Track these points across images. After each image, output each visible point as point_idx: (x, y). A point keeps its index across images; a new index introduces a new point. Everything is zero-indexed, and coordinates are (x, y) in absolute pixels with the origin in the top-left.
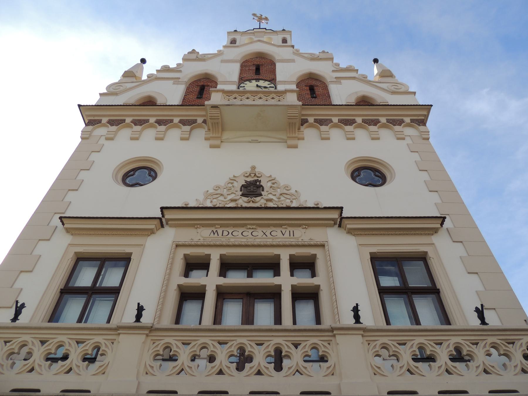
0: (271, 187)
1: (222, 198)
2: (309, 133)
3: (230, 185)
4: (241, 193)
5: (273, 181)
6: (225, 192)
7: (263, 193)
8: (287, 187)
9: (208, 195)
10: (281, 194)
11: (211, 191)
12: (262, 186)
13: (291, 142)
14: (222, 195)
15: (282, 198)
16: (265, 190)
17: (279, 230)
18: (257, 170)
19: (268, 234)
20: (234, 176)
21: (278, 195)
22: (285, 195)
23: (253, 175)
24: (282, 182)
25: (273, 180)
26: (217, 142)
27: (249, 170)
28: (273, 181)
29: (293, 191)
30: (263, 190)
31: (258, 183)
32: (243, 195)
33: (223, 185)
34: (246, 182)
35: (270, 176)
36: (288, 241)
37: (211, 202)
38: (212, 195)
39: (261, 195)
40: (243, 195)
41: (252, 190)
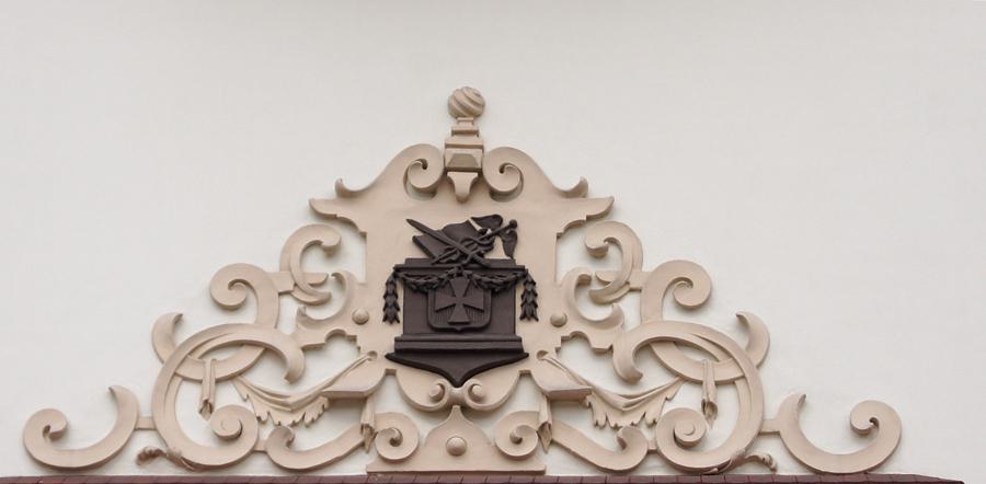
0: (583, 282)
1: (267, 377)
3: (317, 266)
4: (386, 337)
5: (596, 237)
6: (286, 332)
7: (528, 333)
9: (184, 355)
10: (646, 348)
11: (201, 319)
12: (522, 275)
14: (269, 351)
15: (653, 378)
16: (548, 306)
18: (495, 134)
20: (345, 194)
21: (625, 347)
22: (667, 355)
23: (463, 181)
24: (659, 244)
25: (590, 216)
27: (436, 132)
28: (596, 237)
29: (718, 320)
30: (530, 314)
31: (498, 254)
32: (404, 355)
33: (271, 265)
34: (425, 237)
35: (579, 191)
37: (207, 407)
38: (206, 347)
39: (516, 354)
40: (404, 355)
41: (459, 315)
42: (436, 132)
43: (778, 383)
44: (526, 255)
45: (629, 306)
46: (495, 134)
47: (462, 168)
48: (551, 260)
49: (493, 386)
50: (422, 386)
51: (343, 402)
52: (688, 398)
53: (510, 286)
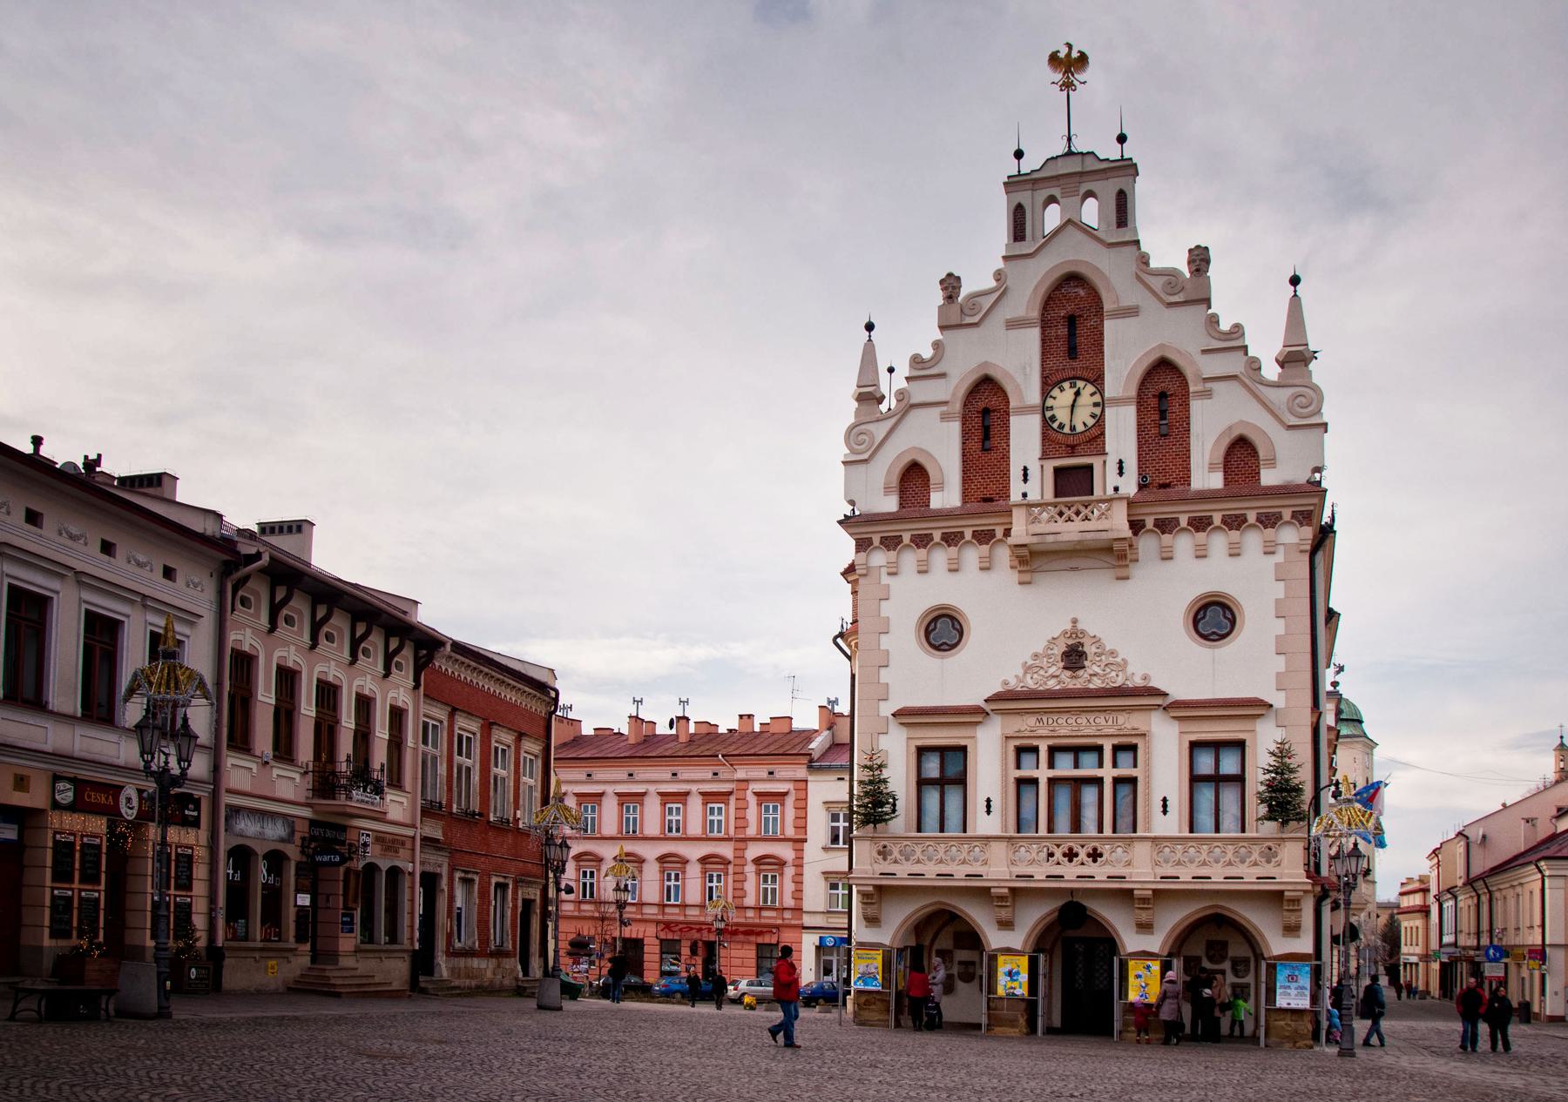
2: (1147, 544)
4: (1061, 664)
8: (1113, 653)
9: (1027, 669)
11: (1030, 662)
13: (1122, 572)
17: (1102, 716)
18: (1080, 626)
25: (1097, 641)
26: (1026, 577)
29: (1119, 660)
38: (1030, 667)
42: (1068, 626)
43: (1130, 669)
46: (1080, 626)
47: (1075, 632)
48: (1090, 649)
49: (1081, 672)
50: (1068, 673)
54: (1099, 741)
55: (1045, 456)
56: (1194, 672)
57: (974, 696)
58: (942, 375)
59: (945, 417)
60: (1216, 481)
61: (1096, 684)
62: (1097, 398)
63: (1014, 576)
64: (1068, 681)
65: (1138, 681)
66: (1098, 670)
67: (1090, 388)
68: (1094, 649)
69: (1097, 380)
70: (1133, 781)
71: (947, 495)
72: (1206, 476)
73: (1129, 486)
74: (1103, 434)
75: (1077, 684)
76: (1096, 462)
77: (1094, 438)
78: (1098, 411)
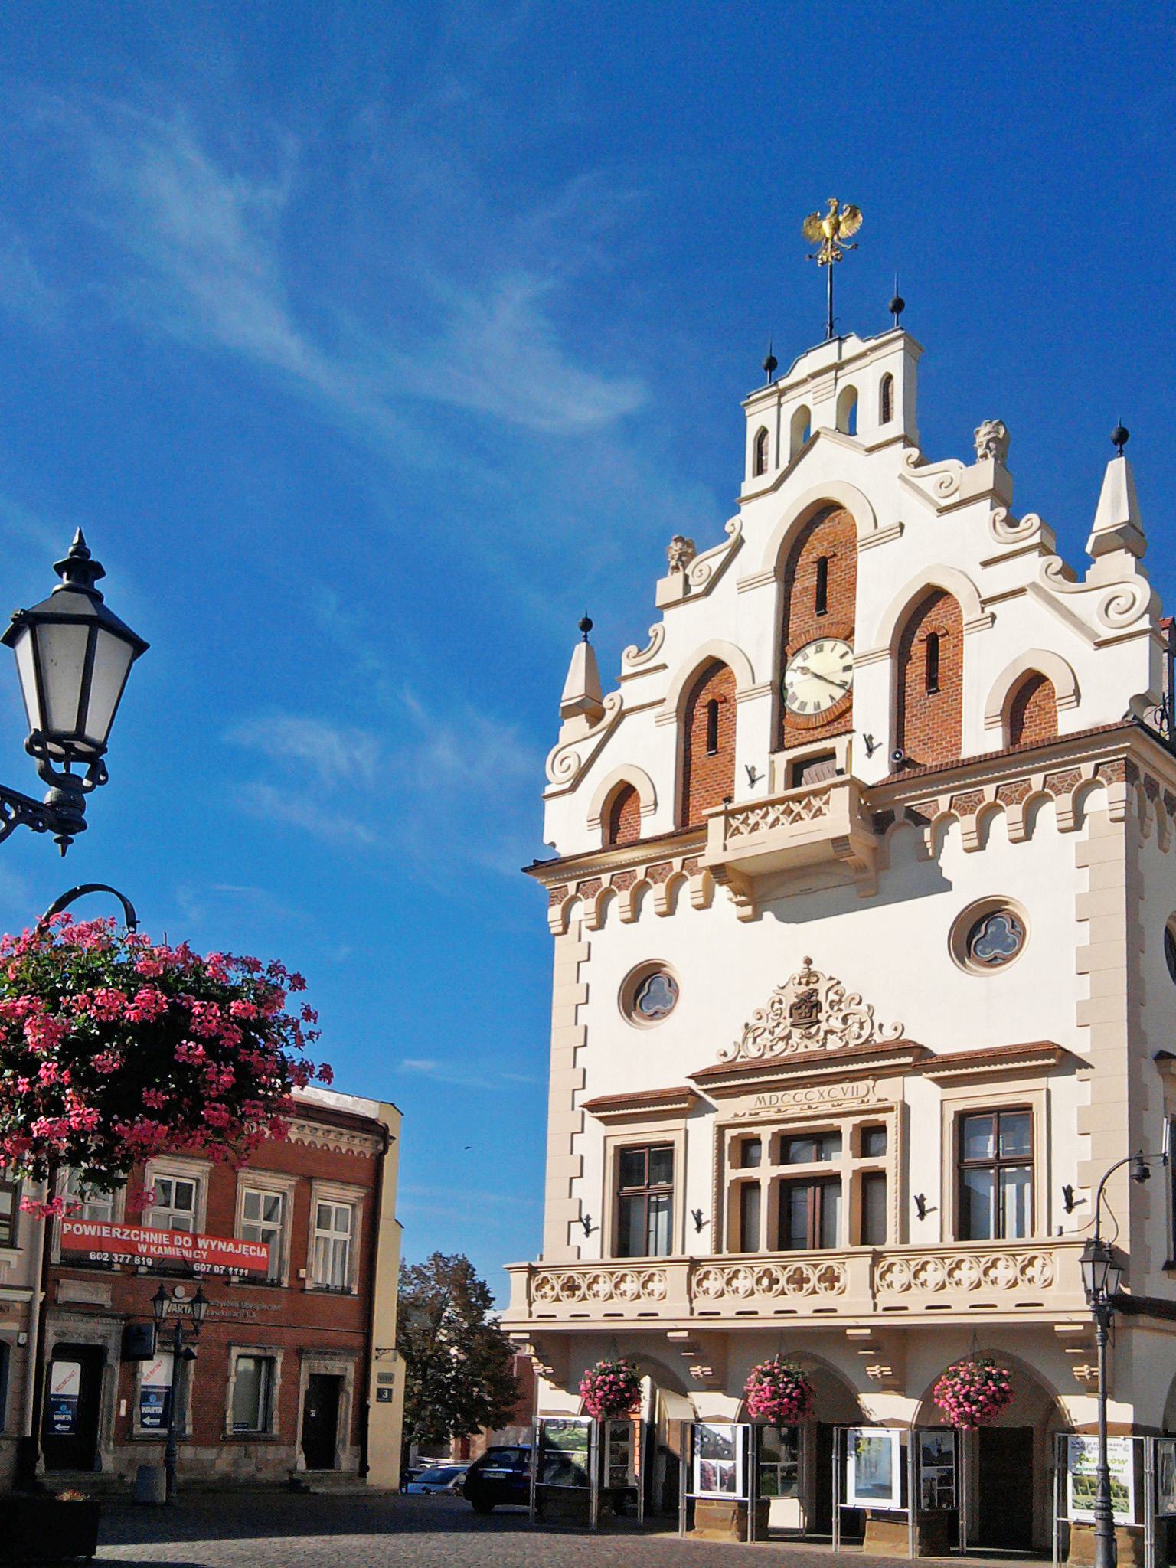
19: (825, 1094)
21: (841, 1015)
26: (748, 910)
36: (855, 1106)
40: (793, 1026)
42: (799, 968)
44: (821, 997)
45: (842, 1006)
49: (813, 1030)
50: (797, 1033)
51: (781, 1039)
52: (856, 1027)
53: (817, 1006)
54: (836, 1122)
55: (779, 744)
56: (967, 1011)
57: (677, 1078)
58: (664, 667)
59: (660, 720)
60: (994, 741)
61: (834, 1044)
62: (849, 660)
63: (735, 911)
64: (802, 1045)
65: (888, 1035)
66: (836, 1024)
67: (842, 647)
68: (832, 996)
69: (848, 636)
70: (880, 1175)
71: (657, 820)
72: (981, 735)
73: (874, 770)
74: (851, 707)
75: (813, 1046)
76: (839, 744)
77: (839, 717)
78: (847, 677)
